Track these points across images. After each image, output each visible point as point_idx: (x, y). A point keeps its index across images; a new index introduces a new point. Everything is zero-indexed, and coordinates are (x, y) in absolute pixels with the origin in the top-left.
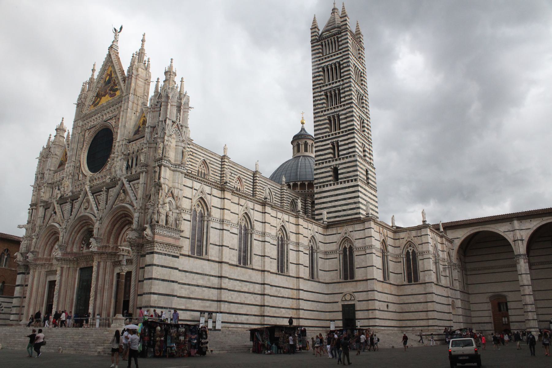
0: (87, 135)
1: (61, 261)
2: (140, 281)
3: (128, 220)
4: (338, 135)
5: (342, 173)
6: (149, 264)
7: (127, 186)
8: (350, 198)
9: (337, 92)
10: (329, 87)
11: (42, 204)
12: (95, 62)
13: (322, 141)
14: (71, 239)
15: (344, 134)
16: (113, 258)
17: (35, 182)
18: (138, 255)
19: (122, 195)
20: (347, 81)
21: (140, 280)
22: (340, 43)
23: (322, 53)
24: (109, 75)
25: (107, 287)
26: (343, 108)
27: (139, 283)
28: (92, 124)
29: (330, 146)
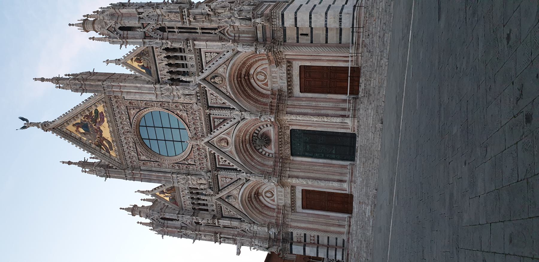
0: (143, 158)
1: (282, 176)
2: (312, 42)
3: (245, 76)
6: (294, 20)
7: (206, 73)
11: (216, 220)
12: (60, 162)
14: (259, 167)
16: (284, 98)
17: (190, 238)
19: (217, 80)
21: (310, 42)
25: (314, 104)
27: (313, 42)
28: (132, 149)
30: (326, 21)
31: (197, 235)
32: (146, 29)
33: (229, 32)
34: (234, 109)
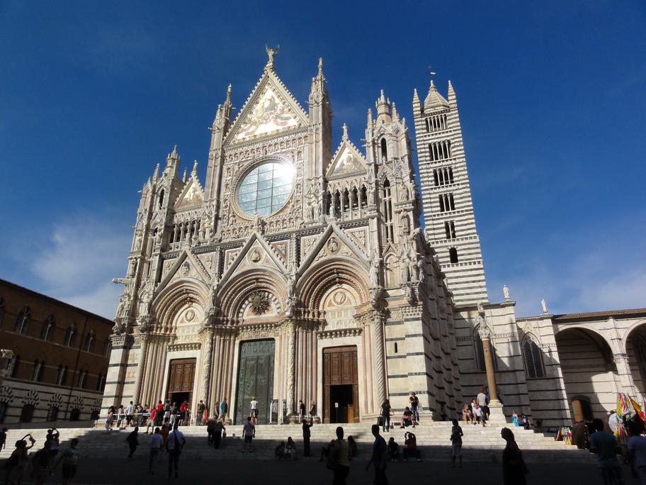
3: (339, 278)
4: (453, 215)
5: (462, 255)
6: (413, 333)
8: (474, 282)
9: (448, 171)
10: (438, 164)
13: (433, 220)
15: (461, 214)
18: (382, 324)
20: (461, 160)
22: (451, 121)
23: (427, 129)
24: (270, 100)
26: (457, 187)
29: (444, 225)
30: (416, 374)
31: (142, 231)
32: (386, 166)
33: (391, 257)
34: (299, 266)
